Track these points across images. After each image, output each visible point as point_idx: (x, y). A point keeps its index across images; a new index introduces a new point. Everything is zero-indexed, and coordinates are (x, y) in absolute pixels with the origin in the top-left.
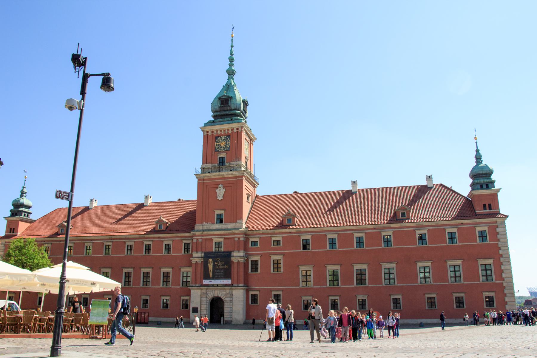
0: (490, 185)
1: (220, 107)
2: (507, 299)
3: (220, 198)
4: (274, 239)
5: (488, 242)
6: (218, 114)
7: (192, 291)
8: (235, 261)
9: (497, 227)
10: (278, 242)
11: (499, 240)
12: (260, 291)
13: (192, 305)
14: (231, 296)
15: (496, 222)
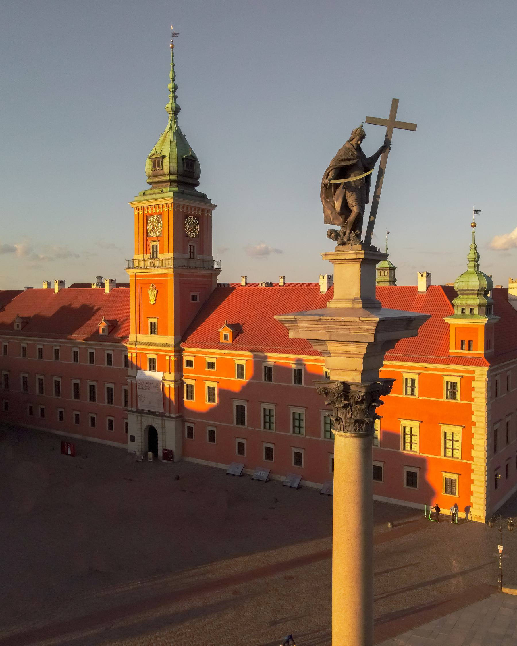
0: (476, 311)
1: (152, 171)
2: (473, 488)
3: (152, 302)
4: (208, 360)
5: (459, 401)
6: (151, 180)
7: (129, 415)
8: (167, 386)
9: (473, 378)
10: (211, 365)
11: (473, 400)
12: (195, 423)
13: (131, 432)
14: (164, 427)
15: (473, 372)
